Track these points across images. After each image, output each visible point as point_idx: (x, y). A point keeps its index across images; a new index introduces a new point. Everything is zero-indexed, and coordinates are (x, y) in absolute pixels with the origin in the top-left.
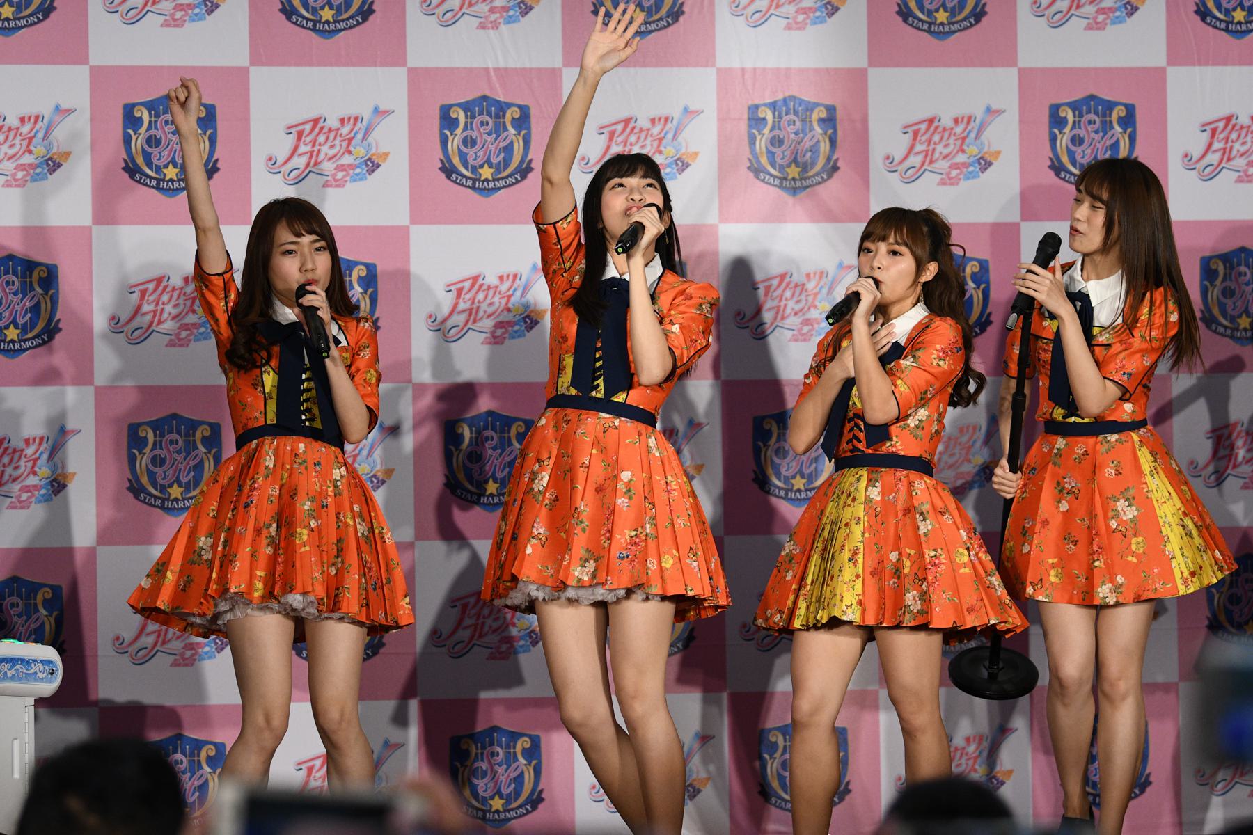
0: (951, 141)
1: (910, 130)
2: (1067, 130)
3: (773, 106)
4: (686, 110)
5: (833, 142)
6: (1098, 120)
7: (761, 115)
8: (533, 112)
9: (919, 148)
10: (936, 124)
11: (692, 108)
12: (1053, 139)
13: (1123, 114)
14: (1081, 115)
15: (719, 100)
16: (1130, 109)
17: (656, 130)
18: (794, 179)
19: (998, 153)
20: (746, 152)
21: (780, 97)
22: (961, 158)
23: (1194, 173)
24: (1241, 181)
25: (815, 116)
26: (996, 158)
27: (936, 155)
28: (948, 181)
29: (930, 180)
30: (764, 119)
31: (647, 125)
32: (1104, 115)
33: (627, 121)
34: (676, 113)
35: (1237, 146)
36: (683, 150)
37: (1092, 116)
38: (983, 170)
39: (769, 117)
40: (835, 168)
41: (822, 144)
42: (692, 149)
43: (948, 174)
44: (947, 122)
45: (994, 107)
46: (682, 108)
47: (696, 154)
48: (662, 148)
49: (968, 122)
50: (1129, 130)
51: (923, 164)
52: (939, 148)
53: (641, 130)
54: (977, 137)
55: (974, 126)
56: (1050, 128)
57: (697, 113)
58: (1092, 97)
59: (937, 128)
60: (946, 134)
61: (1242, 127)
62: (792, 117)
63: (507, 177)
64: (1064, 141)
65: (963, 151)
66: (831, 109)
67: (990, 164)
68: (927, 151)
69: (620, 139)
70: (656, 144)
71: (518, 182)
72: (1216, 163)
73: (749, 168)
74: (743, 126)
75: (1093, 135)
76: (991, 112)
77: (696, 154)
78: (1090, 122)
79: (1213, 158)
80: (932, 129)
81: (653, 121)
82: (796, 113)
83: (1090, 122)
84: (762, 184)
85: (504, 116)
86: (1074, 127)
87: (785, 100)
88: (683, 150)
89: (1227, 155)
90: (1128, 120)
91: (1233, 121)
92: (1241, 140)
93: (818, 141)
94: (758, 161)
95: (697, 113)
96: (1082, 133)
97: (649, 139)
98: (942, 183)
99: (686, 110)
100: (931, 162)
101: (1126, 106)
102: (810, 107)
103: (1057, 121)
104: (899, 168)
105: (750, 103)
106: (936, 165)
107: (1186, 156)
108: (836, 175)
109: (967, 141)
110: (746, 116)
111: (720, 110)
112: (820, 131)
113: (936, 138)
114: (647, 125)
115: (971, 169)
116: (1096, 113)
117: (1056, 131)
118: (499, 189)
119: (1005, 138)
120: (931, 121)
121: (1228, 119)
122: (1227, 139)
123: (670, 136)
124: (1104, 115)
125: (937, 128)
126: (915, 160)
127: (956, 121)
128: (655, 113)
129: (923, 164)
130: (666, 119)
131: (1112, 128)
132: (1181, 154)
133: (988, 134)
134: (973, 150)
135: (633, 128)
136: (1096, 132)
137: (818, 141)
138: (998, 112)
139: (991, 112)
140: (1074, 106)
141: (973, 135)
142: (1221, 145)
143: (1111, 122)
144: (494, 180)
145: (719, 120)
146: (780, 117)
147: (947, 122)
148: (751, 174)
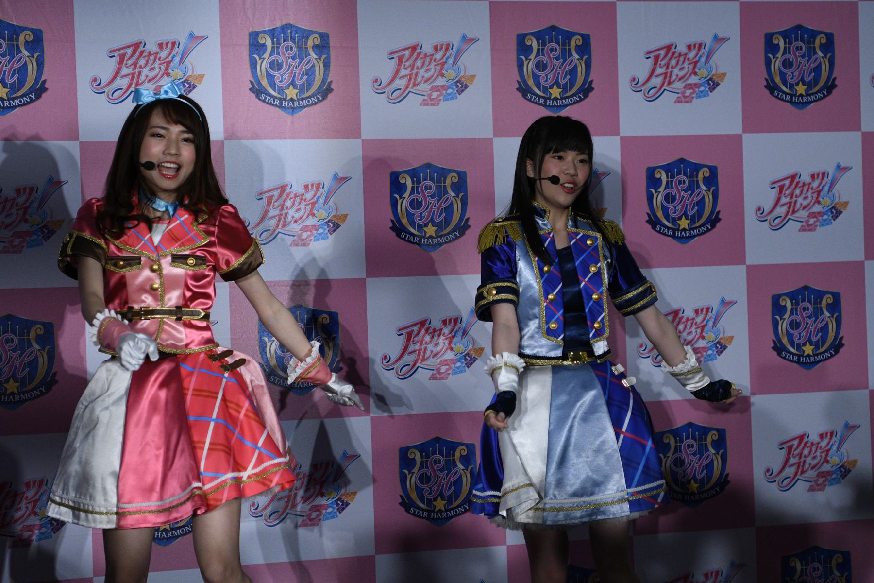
0: (432, 66)
1: (395, 56)
2: (532, 56)
3: (272, 33)
4: (191, 35)
5: (327, 65)
6: (558, 48)
7: (262, 42)
8: (45, 36)
9: (403, 72)
10: (418, 50)
11: (197, 34)
12: (520, 65)
13: (580, 43)
14: (544, 44)
15: (222, 27)
16: (586, 38)
17: (163, 54)
18: (292, 100)
19: (473, 77)
20: (249, 76)
21: (278, 25)
22: (441, 81)
23: (641, 94)
24: (680, 102)
25: (310, 43)
26: (472, 81)
27: (419, 79)
28: (429, 102)
29: (413, 100)
30: (264, 45)
31: (155, 49)
32: (564, 44)
33: (136, 46)
34: (183, 39)
35: (676, 71)
36: (190, 73)
37: (554, 45)
38: (460, 92)
39: (269, 43)
40: (329, 90)
41: (317, 68)
42: (198, 72)
43: (430, 95)
44: (428, 49)
45: (469, 36)
46: (187, 34)
47: (202, 76)
48: (170, 71)
49: (447, 49)
50: (585, 57)
51: (407, 87)
52: (422, 72)
53: (150, 54)
54: (455, 62)
55: (452, 52)
56: (518, 55)
57: (202, 38)
58: (553, 28)
59: (419, 54)
60: (427, 60)
61: (680, 55)
62: (290, 43)
63: (22, 96)
64: (529, 67)
65: (443, 75)
66: (324, 37)
67: (466, 87)
68: (411, 75)
69: (129, 62)
70: (163, 67)
71: (32, 101)
72: (658, 86)
73: (250, 89)
74: (245, 52)
75: (554, 61)
76: (467, 41)
77: (202, 76)
78: (552, 50)
79: (656, 81)
80: (415, 55)
81: (161, 45)
82: (293, 39)
83: (552, 50)
84: (263, 104)
85: (17, 40)
86: (538, 55)
87: (283, 28)
88: (190, 73)
89: (667, 79)
90: (585, 49)
91: (673, 50)
92: (679, 67)
93: (313, 66)
94: (259, 83)
95: (202, 38)
96: (545, 59)
97: (158, 62)
98: (424, 103)
99: (191, 35)
100: (415, 85)
101: (582, 35)
102: (306, 34)
103: (523, 49)
104: (386, 90)
105: (251, 30)
106: (419, 87)
107: (634, 79)
108: (329, 96)
109: (446, 66)
110: (247, 42)
111: (223, 36)
112: (315, 57)
113: (419, 63)
114: (155, 49)
115: (450, 91)
116: (557, 42)
117: (523, 57)
118: (15, 107)
119: (478, 62)
120: (414, 48)
121: (669, 48)
122: (667, 65)
123: (177, 59)
124: (564, 44)
125: (419, 54)
126: (400, 83)
127: (436, 48)
128: (164, 38)
129: (407, 87)
130: (174, 44)
131: (570, 55)
132: (629, 78)
133: (464, 60)
134: (451, 74)
135: (143, 52)
136: (557, 59)
137: (313, 66)
138: (473, 41)
139: (467, 41)
140: (538, 36)
141: (451, 61)
142: (663, 70)
143: (569, 49)
144: (9, 99)
145: (223, 45)
146: (279, 43)
147: (428, 49)
148: (253, 96)
